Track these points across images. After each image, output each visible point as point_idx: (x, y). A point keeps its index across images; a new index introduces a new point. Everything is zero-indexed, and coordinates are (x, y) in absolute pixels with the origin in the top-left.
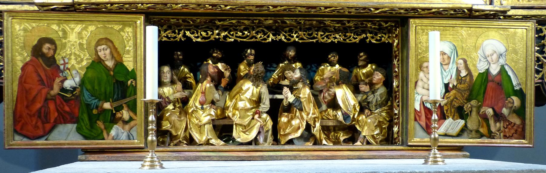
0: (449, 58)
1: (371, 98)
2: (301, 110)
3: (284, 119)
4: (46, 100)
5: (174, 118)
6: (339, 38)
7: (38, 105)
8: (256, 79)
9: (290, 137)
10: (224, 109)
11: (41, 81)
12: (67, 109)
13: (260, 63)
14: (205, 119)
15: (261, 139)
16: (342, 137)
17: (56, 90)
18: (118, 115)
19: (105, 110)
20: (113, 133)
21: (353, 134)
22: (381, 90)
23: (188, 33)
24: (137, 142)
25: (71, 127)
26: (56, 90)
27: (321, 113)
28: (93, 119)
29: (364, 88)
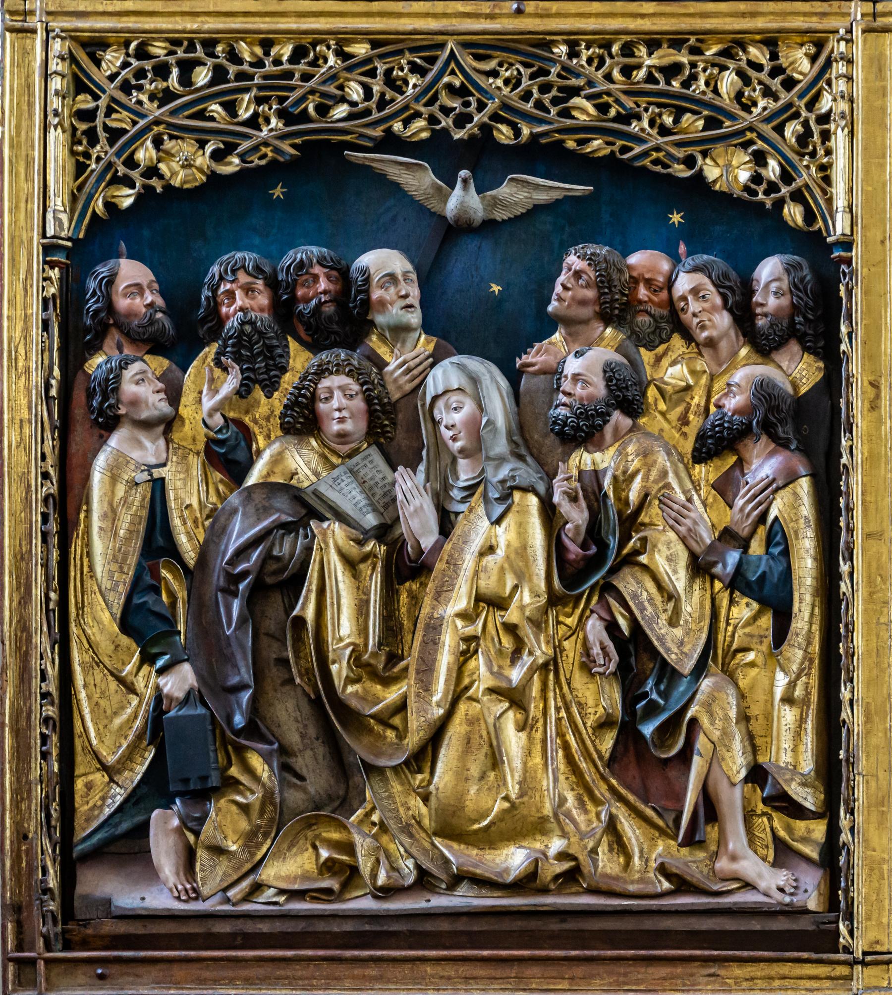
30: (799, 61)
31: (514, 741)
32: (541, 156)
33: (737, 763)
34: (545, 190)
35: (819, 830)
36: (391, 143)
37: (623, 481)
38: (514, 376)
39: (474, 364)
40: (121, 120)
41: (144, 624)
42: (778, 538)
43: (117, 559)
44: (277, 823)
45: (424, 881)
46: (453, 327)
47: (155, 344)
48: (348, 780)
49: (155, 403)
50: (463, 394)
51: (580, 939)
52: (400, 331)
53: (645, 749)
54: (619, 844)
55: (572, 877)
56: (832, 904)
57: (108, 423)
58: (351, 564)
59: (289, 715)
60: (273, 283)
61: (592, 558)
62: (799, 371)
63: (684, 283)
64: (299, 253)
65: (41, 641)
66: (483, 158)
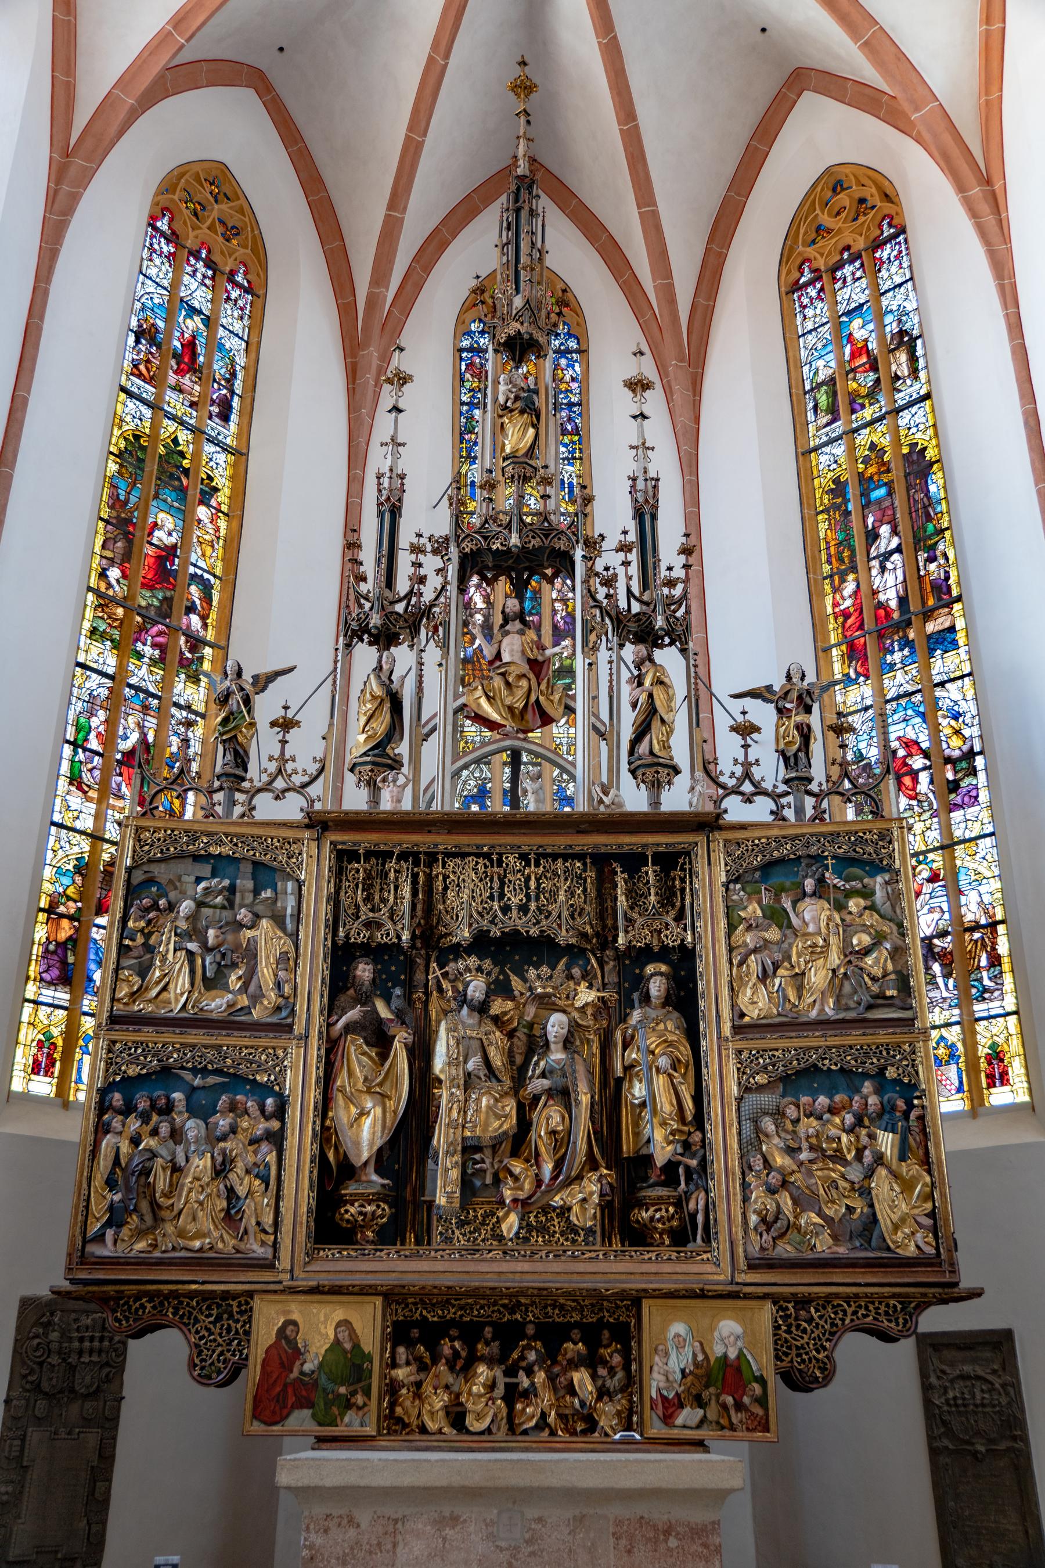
0: (685, 1340)
1: (609, 1383)
2: (536, 1396)
3: (519, 1406)
4: (285, 1385)
5: (408, 1403)
6: (576, 1317)
7: (278, 1389)
8: (490, 1362)
9: (525, 1427)
10: (458, 1395)
11: (282, 1364)
12: (304, 1393)
13: (497, 1343)
14: (439, 1405)
15: (494, 1430)
16: (580, 1427)
17: (295, 1374)
18: (353, 1400)
19: (339, 1395)
20: (346, 1419)
21: (592, 1425)
22: (620, 1374)
23: (424, 1313)
24: (370, 1430)
25: (307, 1413)
26: (295, 1374)
27: (557, 1400)
28: (328, 1405)
29: (602, 1372)
30: (280, 1053)
31: (200, 1214)
32: (218, 1072)
33: (253, 1222)
34: (218, 1079)
35: (272, 1238)
36: (183, 1068)
37: (231, 1151)
38: (207, 1124)
39: (198, 1121)
40: (118, 1060)
41: (111, 1183)
42: (267, 1166)
43: (106, 1167)
44: (140, 1234)
45: (174, 1249)
46: (193, 1111)
47: (120, 1113)
48: (158, 1220)
49: (120, 1128)
50: (193, 1128)
51: (212, 1265)
52: (180, 1112)
53: (231, 1217)
54: (223, 1241)
55: (211, 1249)
56: (274, 1257)
57: (108, 1132)
58: (164, 1169)
59: (144, 1206)
60: (151, 1100)
61: (221, 1170)
62: (275, 1125)
63: (249, 1104)
64: (156, 1094)
65: (85, 1186)
66: (204, 1071)
